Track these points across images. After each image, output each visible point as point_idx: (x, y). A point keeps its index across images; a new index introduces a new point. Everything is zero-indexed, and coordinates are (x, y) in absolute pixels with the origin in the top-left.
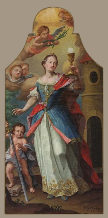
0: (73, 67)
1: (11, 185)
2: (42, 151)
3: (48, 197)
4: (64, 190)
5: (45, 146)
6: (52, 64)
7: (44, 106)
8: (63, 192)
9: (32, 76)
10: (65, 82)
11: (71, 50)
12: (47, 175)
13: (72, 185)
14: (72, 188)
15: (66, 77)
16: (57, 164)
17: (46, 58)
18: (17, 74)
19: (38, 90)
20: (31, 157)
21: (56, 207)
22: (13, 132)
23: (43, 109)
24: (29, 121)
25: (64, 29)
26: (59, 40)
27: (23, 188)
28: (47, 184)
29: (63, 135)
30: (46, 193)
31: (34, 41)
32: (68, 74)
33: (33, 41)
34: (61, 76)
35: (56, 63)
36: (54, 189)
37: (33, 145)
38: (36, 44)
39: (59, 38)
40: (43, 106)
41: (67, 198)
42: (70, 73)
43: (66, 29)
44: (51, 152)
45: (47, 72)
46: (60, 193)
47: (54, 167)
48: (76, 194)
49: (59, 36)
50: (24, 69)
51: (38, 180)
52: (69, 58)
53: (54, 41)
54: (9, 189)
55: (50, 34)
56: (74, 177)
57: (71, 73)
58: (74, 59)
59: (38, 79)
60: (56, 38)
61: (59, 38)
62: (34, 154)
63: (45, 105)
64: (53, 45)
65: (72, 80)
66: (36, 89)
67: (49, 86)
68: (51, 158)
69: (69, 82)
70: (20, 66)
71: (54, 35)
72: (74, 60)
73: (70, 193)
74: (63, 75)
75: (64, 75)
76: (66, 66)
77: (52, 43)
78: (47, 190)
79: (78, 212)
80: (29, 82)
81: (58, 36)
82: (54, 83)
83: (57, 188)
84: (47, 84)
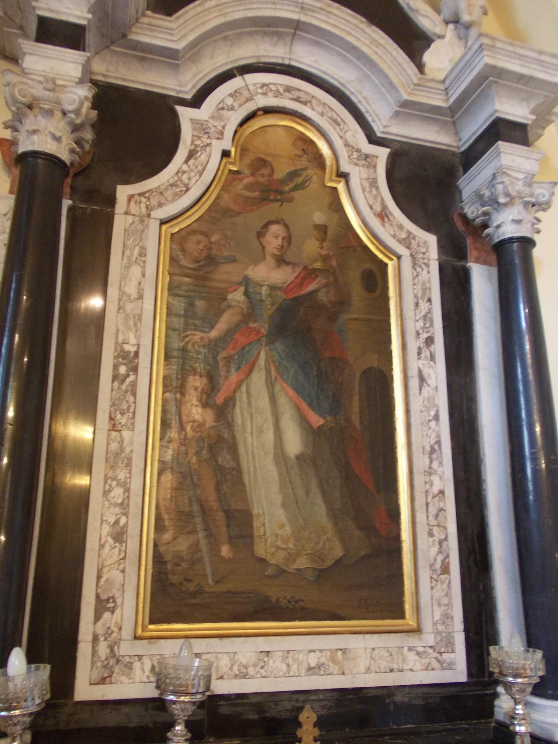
0: (324, 252)
1: (167, 536)
2: (255, 445)
3: (269, 572)
4: (309, 551)
5: (261, 431)
6: (279, 241)
7: (261, 332)
8: (305, 557)
9: (232, 260)
10: (308, 285)
11: (319, 218)
12: (265, 510)
13: (328, 540)
14: (327, 546)
15: (309, 274)
16: (291, 482)
17: (266, 226)
18: (198, 250)
19: (246, 293)
20: (225, 459)
21: (289, 602)
22: (182, 389)
23: (259, 339)
24: (224, 365)
25: (304, 174)
26: (295, 194)
27: (203, 545)
28: (265, 534)
29: (304, 406)
30: (262, 561)
31: (240, 187)
32: (315, 267)
33: (239, 187)
34: (298, 270)
35: (288, 239)
36: (284, 549)
37: (230, 425)
38: (244, 191)
39: (292, 190)
40: (258, 332)
41: (316, 573)
42: (318, 265)
43: (310, 172)
44: (275, 447)
45: (268, 257)
46: (298, 561)
47: (282, 487)
48: (338, 562)
49: (296, 186)
50: (215, 243)
51: (240, 524)
52: (315, 232)
53: (284, 193)
54: (162, 549)
55: (275, 177)
56: (334, 515)
57: (320, 266)
58: (326, 238)
59: (246, 269)
60: (287, 188)
61: (292, 190)
62: (233, 450)
63: (263, 331)
64: (282, 201)
65: (324, 281)
66: (242, 289)
67: (273, 288)
68: (277, 464)
69: (317, 284)
70: (206, 235)
71: (283, 182)
72: (328, 239)
73: (323, 560)
74: (302, 267)
75: (305, 268)
76: (311, 248)
77: (279, 197)
78: (266, 552)
79: (343, 615)
80: (226, 273)
81: (292, 185)
82: (285, 283)
83: (291, 546)
84: (267, 283)
